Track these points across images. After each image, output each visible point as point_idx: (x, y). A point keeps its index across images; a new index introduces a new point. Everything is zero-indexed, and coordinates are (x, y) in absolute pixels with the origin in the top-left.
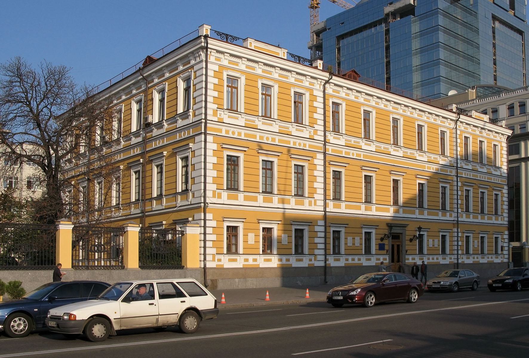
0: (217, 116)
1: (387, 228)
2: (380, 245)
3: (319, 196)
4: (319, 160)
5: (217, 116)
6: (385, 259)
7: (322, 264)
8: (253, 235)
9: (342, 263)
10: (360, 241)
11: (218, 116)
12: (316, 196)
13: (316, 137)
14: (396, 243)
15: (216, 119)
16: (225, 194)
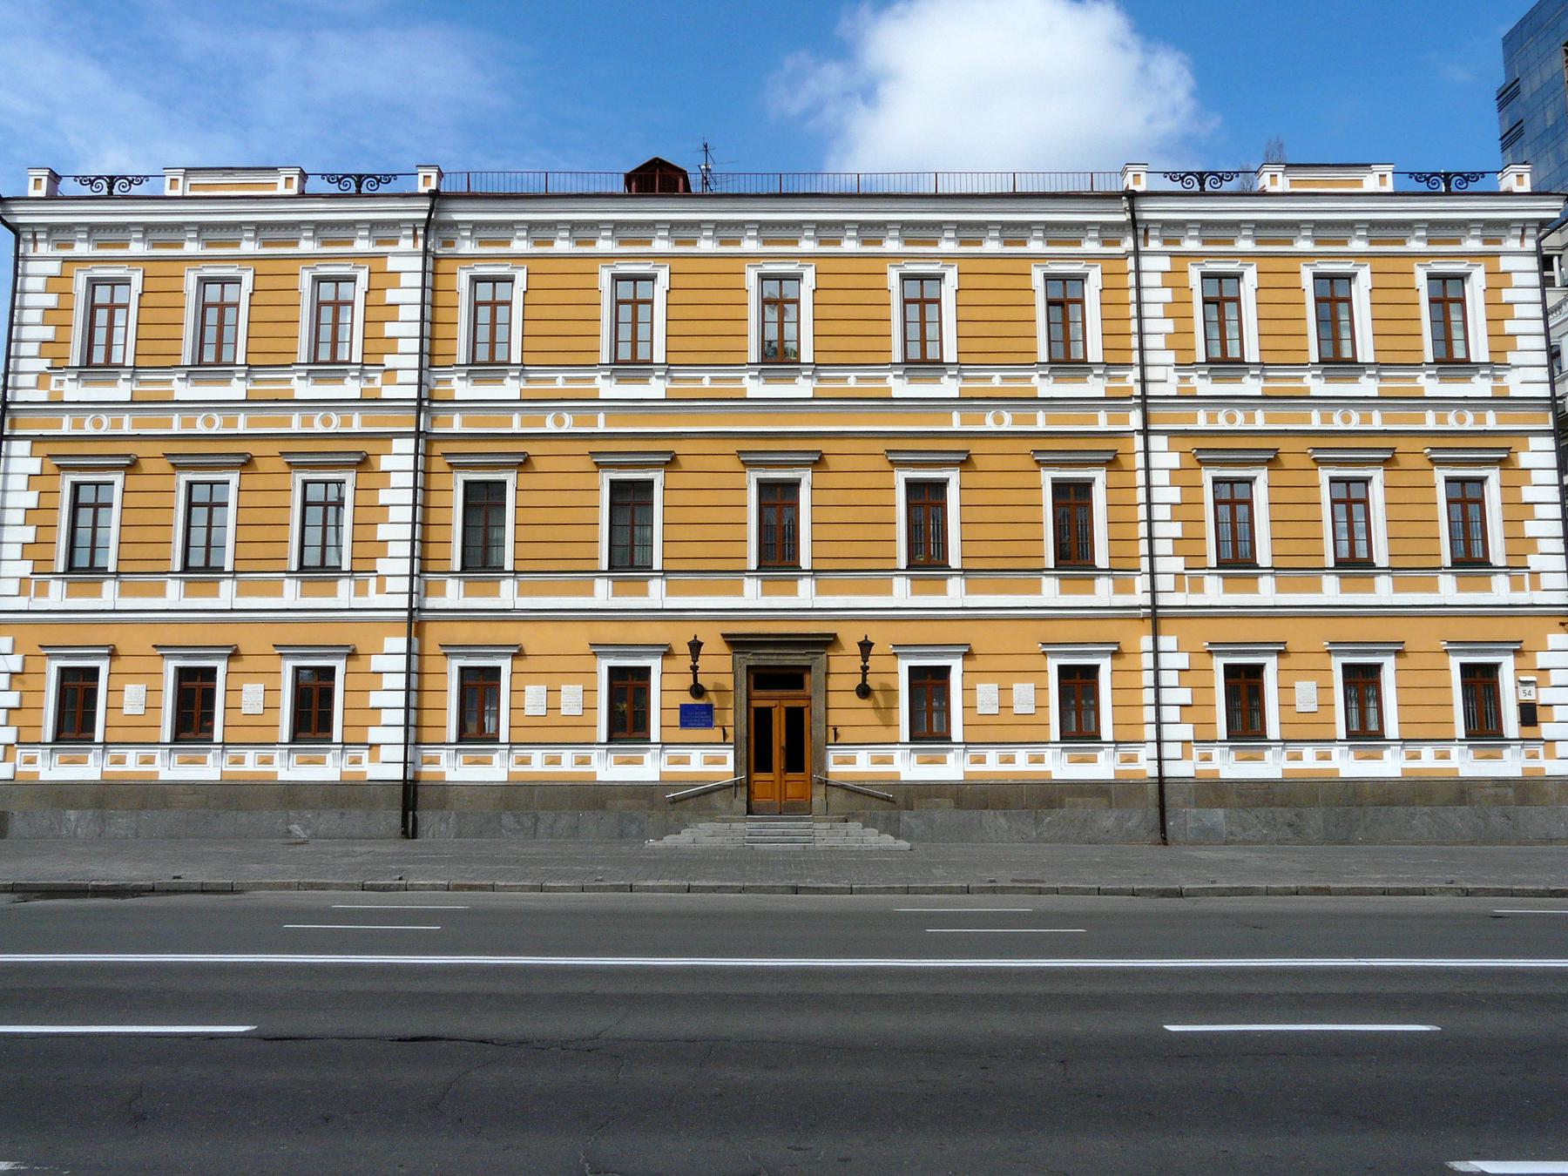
0: (46, 387)
1: (725, 649)
2: (685, 710)
3: (396, 563)
4: (399, 459)
5: (46, 387)
6: (711, 761)
7: (397, 773)
8: (142, 688)
9: (497, 769)
10: (585, 698)
11: (53, 388)
12: (382, 566)
13: (388, 392)
14: (777, 702)
15: (42, 395)
16: (56, 587)
